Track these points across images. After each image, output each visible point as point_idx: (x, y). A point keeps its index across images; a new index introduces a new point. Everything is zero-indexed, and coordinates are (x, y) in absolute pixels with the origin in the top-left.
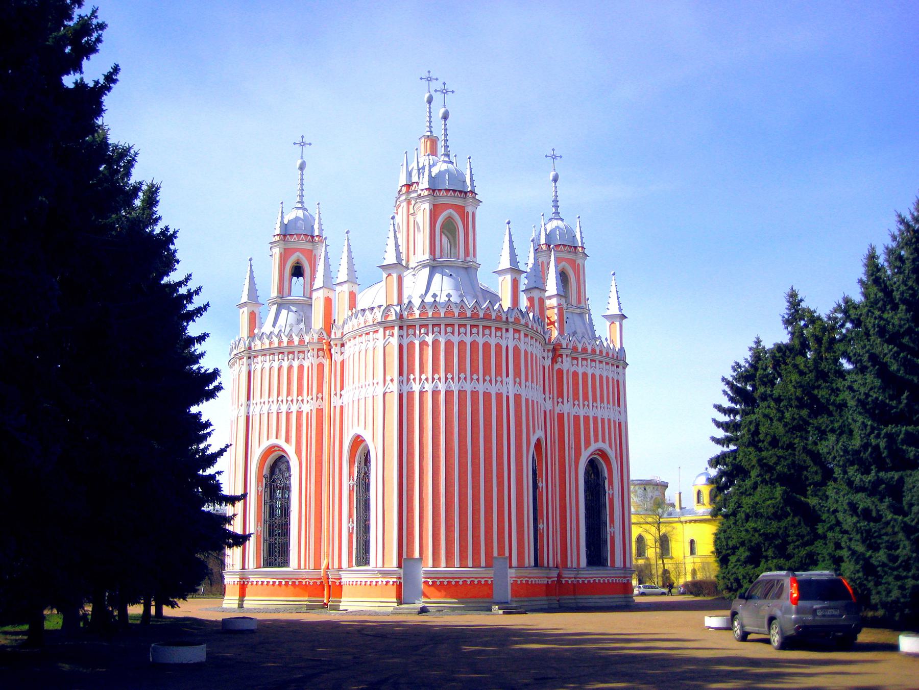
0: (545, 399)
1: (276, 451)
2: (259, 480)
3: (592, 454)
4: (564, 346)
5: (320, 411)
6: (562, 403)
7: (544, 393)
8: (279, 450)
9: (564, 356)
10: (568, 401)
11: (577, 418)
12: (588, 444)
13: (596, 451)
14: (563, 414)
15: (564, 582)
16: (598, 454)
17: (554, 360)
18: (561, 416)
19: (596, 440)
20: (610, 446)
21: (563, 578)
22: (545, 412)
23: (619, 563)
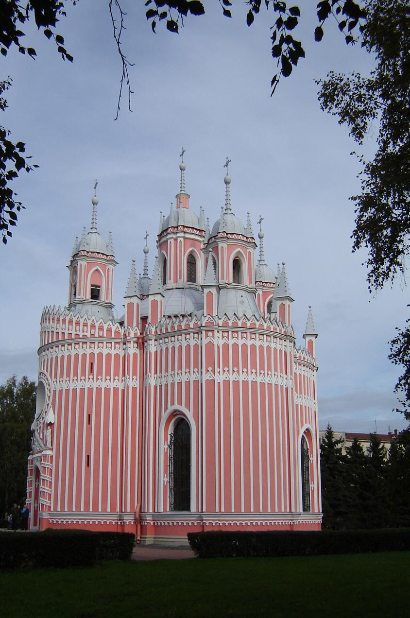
12: (166, 408)
16: (180, 414)
19: (173, 403)
20: (188, 406)
21: (144, 520)
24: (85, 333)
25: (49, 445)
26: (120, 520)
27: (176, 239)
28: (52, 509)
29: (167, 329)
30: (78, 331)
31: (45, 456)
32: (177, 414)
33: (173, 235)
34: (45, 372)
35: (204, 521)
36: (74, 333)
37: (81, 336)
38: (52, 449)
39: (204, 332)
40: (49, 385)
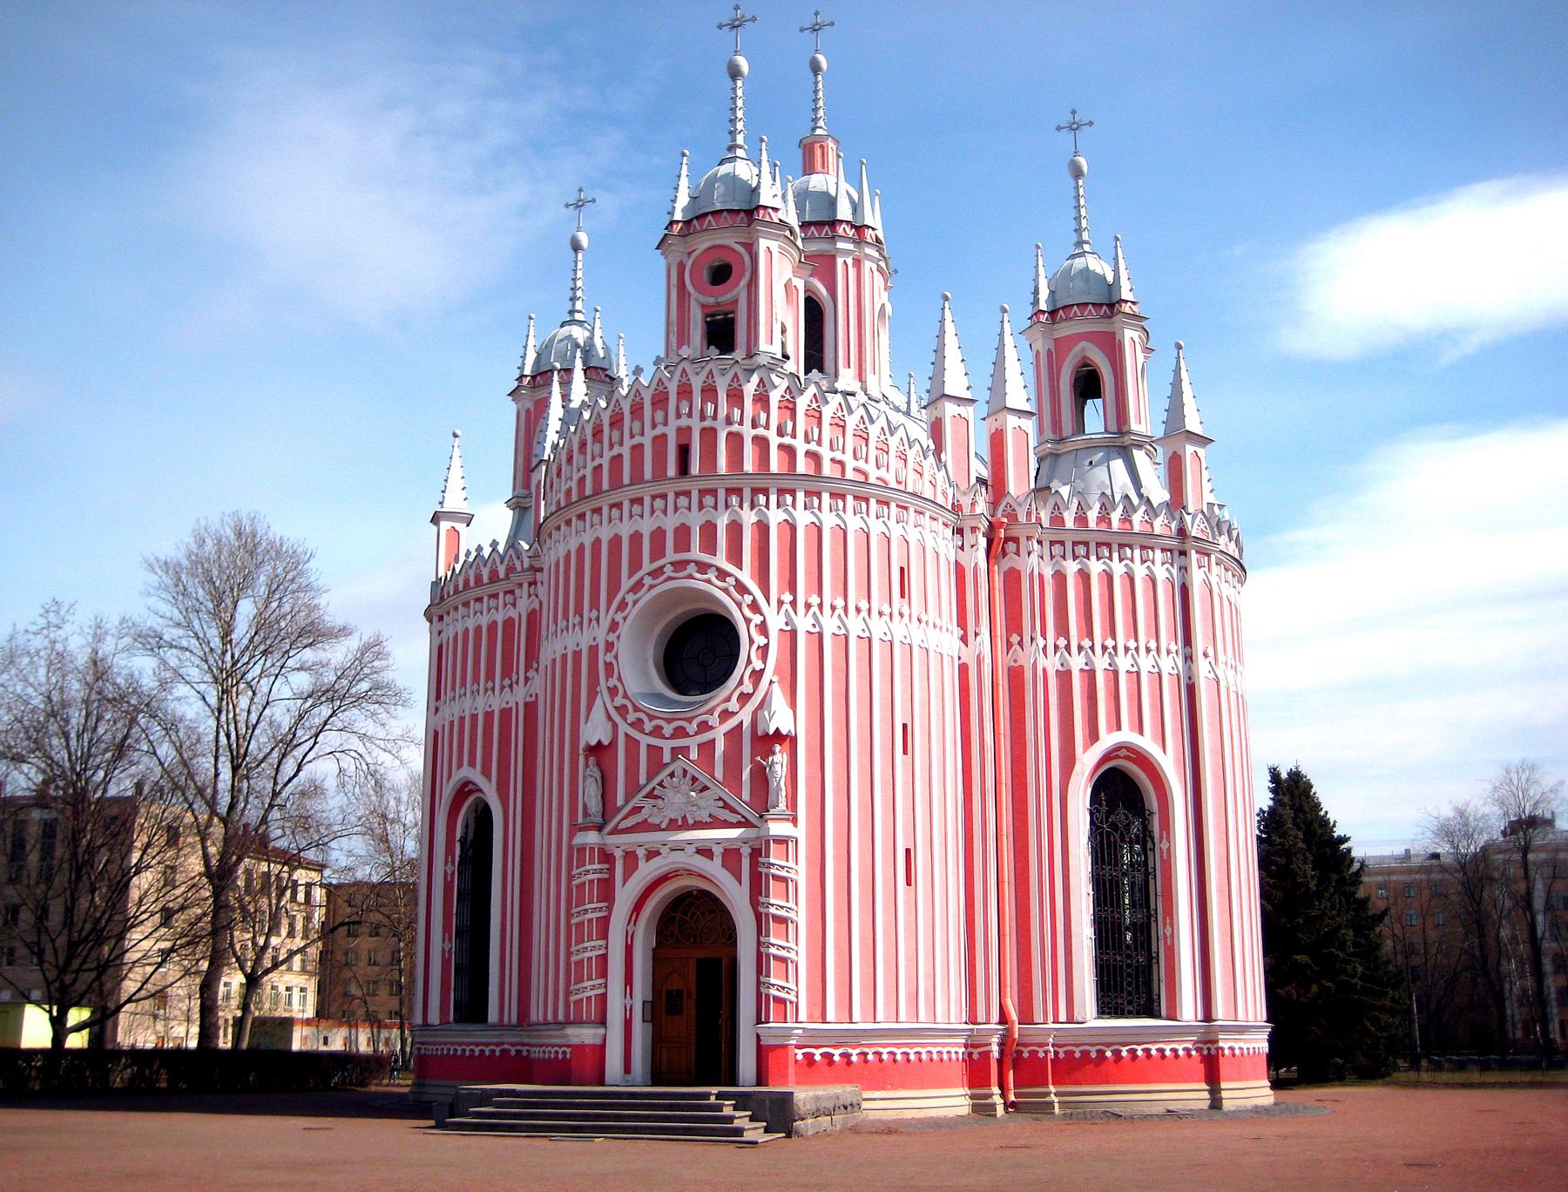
0: (964, 639)
1: (471, 792)
2: (449, 850)
3: (1107, 757)
4: (1022, 518)
5: (531, 708)
6: (1020, 643)
7: (962, 623)
8: (477, 791)
9: (1023, 541)
10: (1032, 639)
11: (1065, 677)
12: (1093, 736)
13: (1118, 748)
14: (1022, 667)
15: (1026, 1055)
17: (994, 550)
18: (1016, 676)
22: (963, 669)
23: (1189, 1010)
24: (882, 473)
25: (782, 805)
26: (973, 1046)
27: (858, 263)
28: (803, 1016)
29: (1081, 519)
30: (884, 470)
31: (782, 841)
32: (1117, 757)
33: (850, 246)
34: (721, 560)
35: (1221, 1044)
36: (850, 464)
37: (872, 480)
38: (795, 821)
39: (1194, 555)
40: (755, 607)
